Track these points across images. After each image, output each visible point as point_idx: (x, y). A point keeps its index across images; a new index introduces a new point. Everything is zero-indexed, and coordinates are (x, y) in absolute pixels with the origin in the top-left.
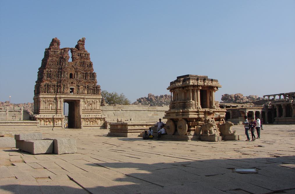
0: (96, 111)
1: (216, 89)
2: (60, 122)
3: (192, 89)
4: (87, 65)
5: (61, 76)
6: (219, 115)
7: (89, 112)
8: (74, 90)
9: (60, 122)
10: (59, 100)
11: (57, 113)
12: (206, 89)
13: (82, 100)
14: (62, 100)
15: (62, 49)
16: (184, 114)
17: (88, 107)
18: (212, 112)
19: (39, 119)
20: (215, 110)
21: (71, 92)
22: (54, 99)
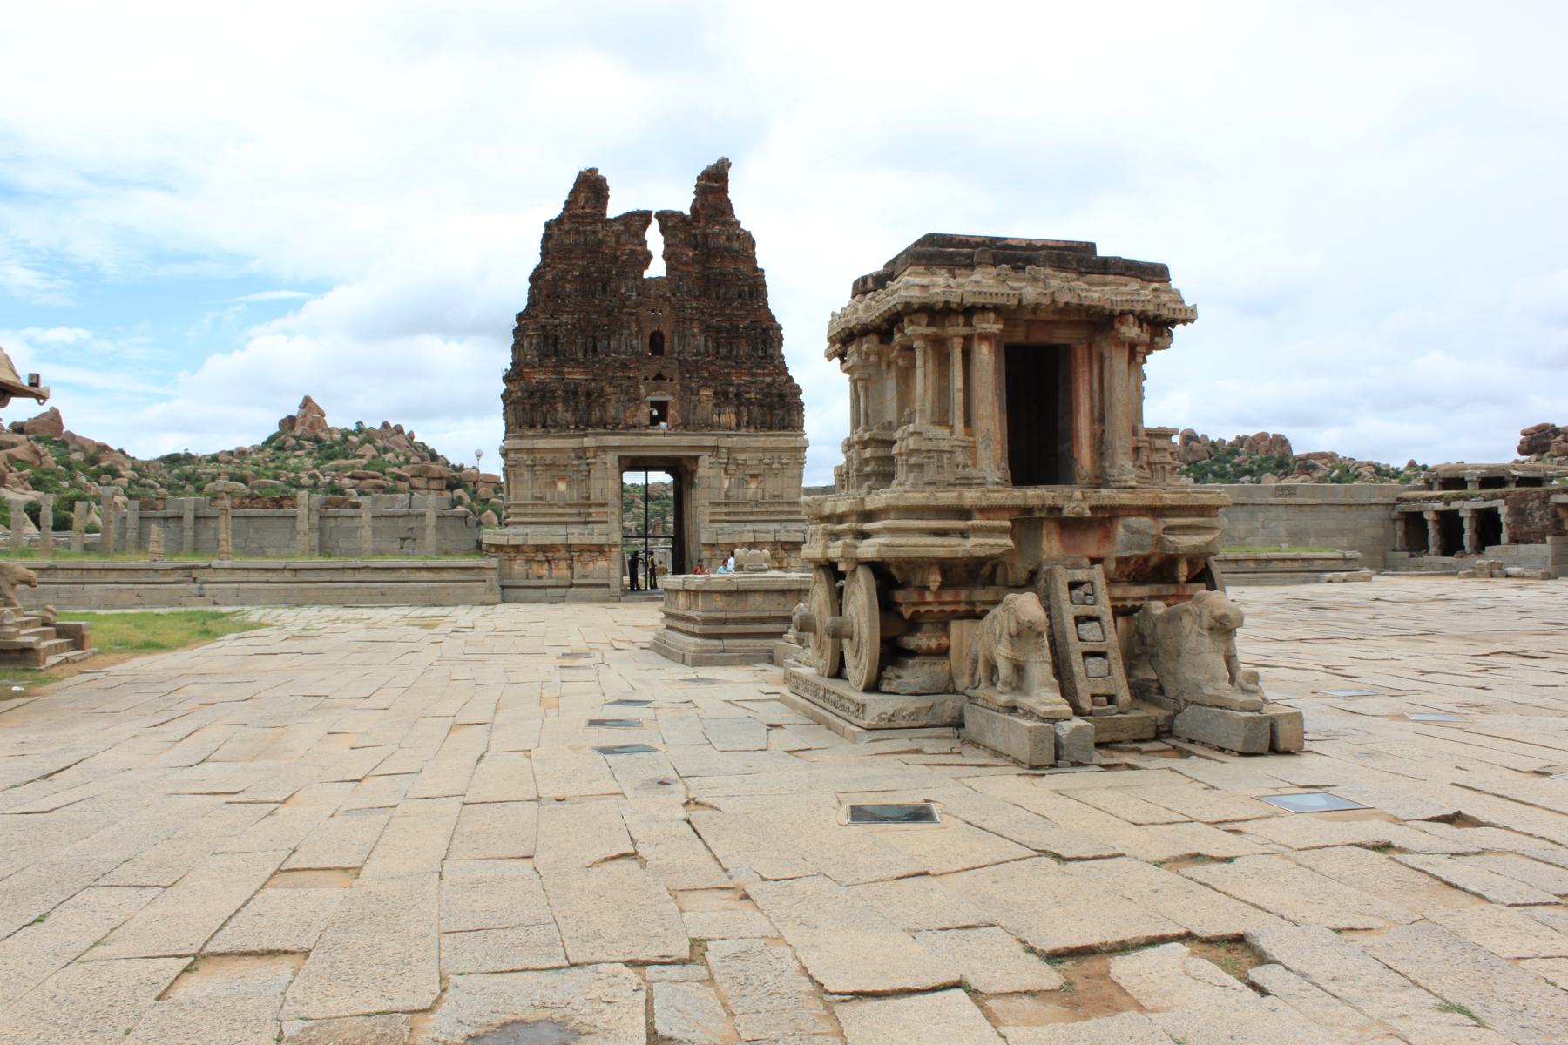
0: (779, 509)
1: (1131, 331)
3: (925, 337)
4: (733, 291)
6: (1159, 541)
7: (745, 513)
8: (671, 412)
12: (1060, 337)
13: (705, 460)
14: (611, 459)
15: (616, 219)
16: (867, 526)
18: (1088, 514)
19: (499, 548)
20: (1125, 498)
21: (655, 421)
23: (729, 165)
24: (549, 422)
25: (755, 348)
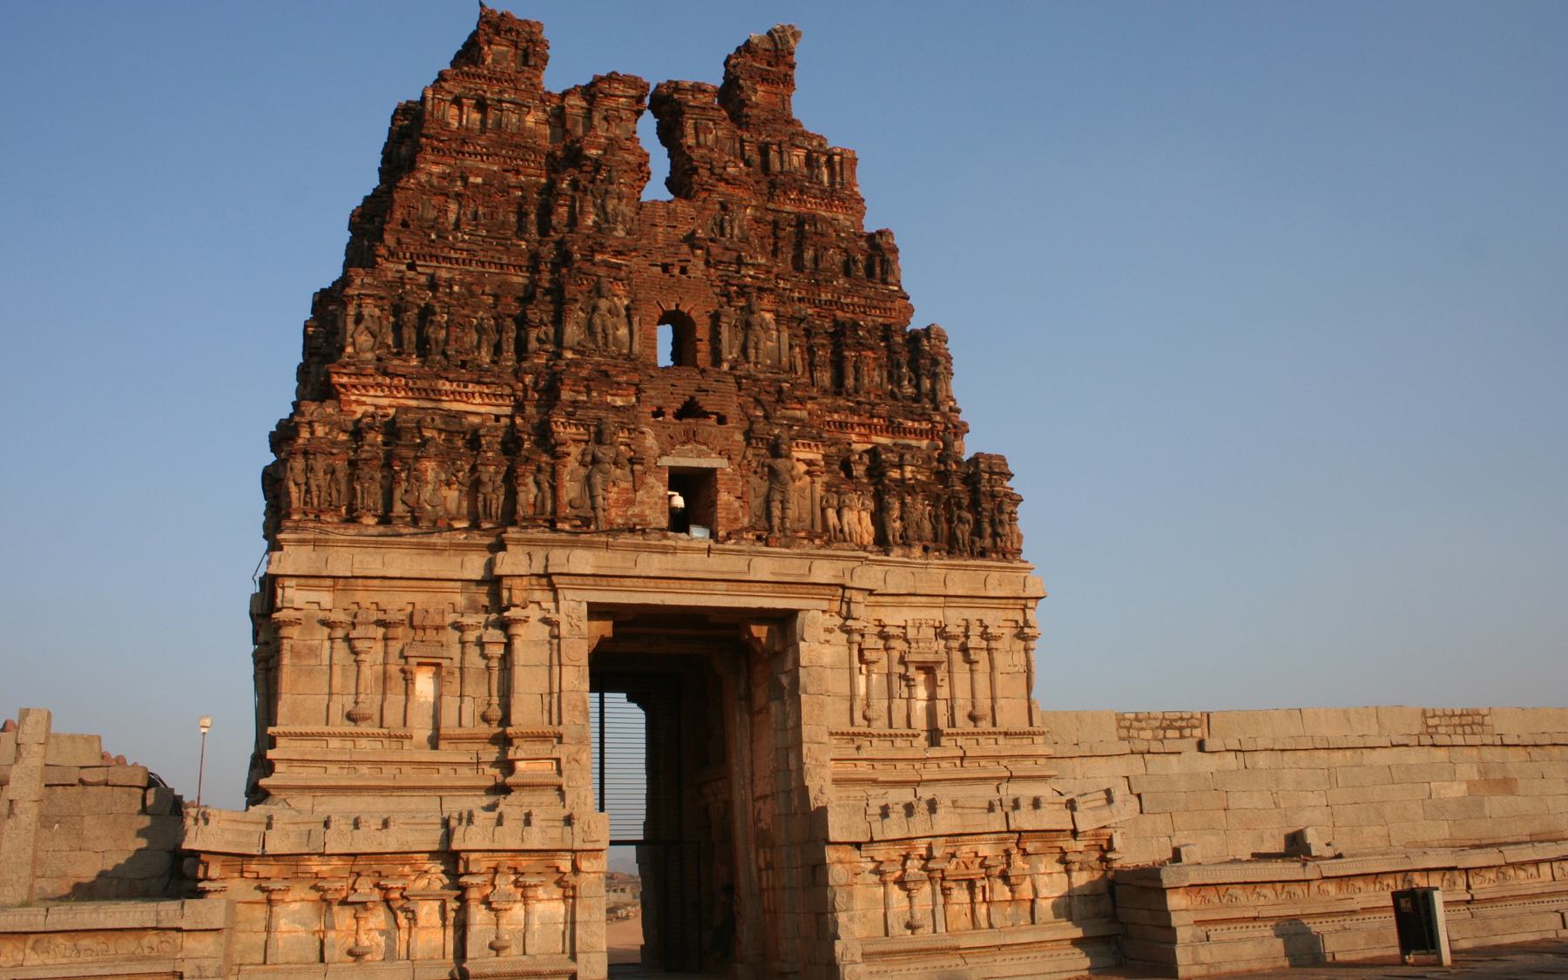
2: (548, 908)
4: (834, 257)
5: (559, 334)
8: (724, 497)
9: (548, 908)
10: (534, 613)
11: (502, 789)
17: (899, 705)
21: (680, 521)
22: (460, 600)
23: (796, 35)
24: (399, 508)
25: (895, 379)
